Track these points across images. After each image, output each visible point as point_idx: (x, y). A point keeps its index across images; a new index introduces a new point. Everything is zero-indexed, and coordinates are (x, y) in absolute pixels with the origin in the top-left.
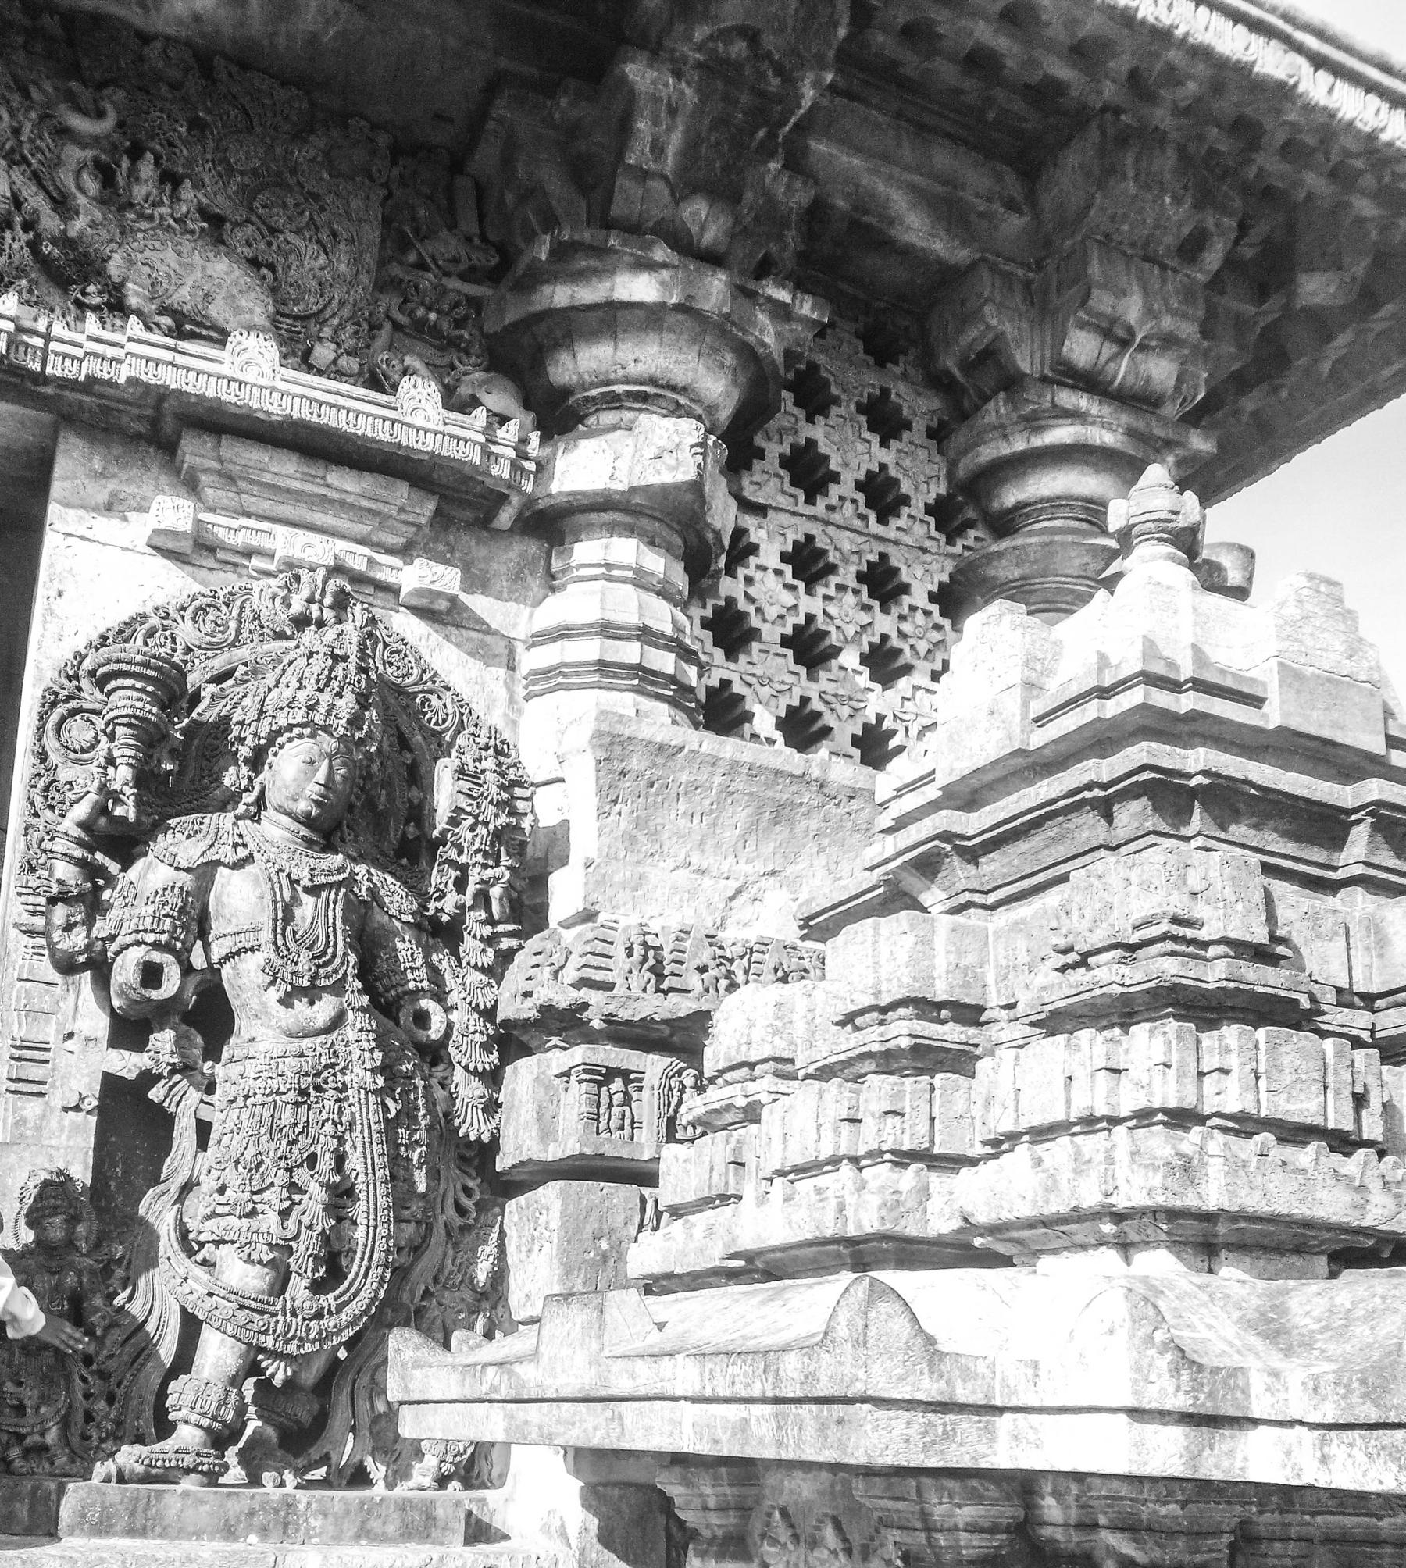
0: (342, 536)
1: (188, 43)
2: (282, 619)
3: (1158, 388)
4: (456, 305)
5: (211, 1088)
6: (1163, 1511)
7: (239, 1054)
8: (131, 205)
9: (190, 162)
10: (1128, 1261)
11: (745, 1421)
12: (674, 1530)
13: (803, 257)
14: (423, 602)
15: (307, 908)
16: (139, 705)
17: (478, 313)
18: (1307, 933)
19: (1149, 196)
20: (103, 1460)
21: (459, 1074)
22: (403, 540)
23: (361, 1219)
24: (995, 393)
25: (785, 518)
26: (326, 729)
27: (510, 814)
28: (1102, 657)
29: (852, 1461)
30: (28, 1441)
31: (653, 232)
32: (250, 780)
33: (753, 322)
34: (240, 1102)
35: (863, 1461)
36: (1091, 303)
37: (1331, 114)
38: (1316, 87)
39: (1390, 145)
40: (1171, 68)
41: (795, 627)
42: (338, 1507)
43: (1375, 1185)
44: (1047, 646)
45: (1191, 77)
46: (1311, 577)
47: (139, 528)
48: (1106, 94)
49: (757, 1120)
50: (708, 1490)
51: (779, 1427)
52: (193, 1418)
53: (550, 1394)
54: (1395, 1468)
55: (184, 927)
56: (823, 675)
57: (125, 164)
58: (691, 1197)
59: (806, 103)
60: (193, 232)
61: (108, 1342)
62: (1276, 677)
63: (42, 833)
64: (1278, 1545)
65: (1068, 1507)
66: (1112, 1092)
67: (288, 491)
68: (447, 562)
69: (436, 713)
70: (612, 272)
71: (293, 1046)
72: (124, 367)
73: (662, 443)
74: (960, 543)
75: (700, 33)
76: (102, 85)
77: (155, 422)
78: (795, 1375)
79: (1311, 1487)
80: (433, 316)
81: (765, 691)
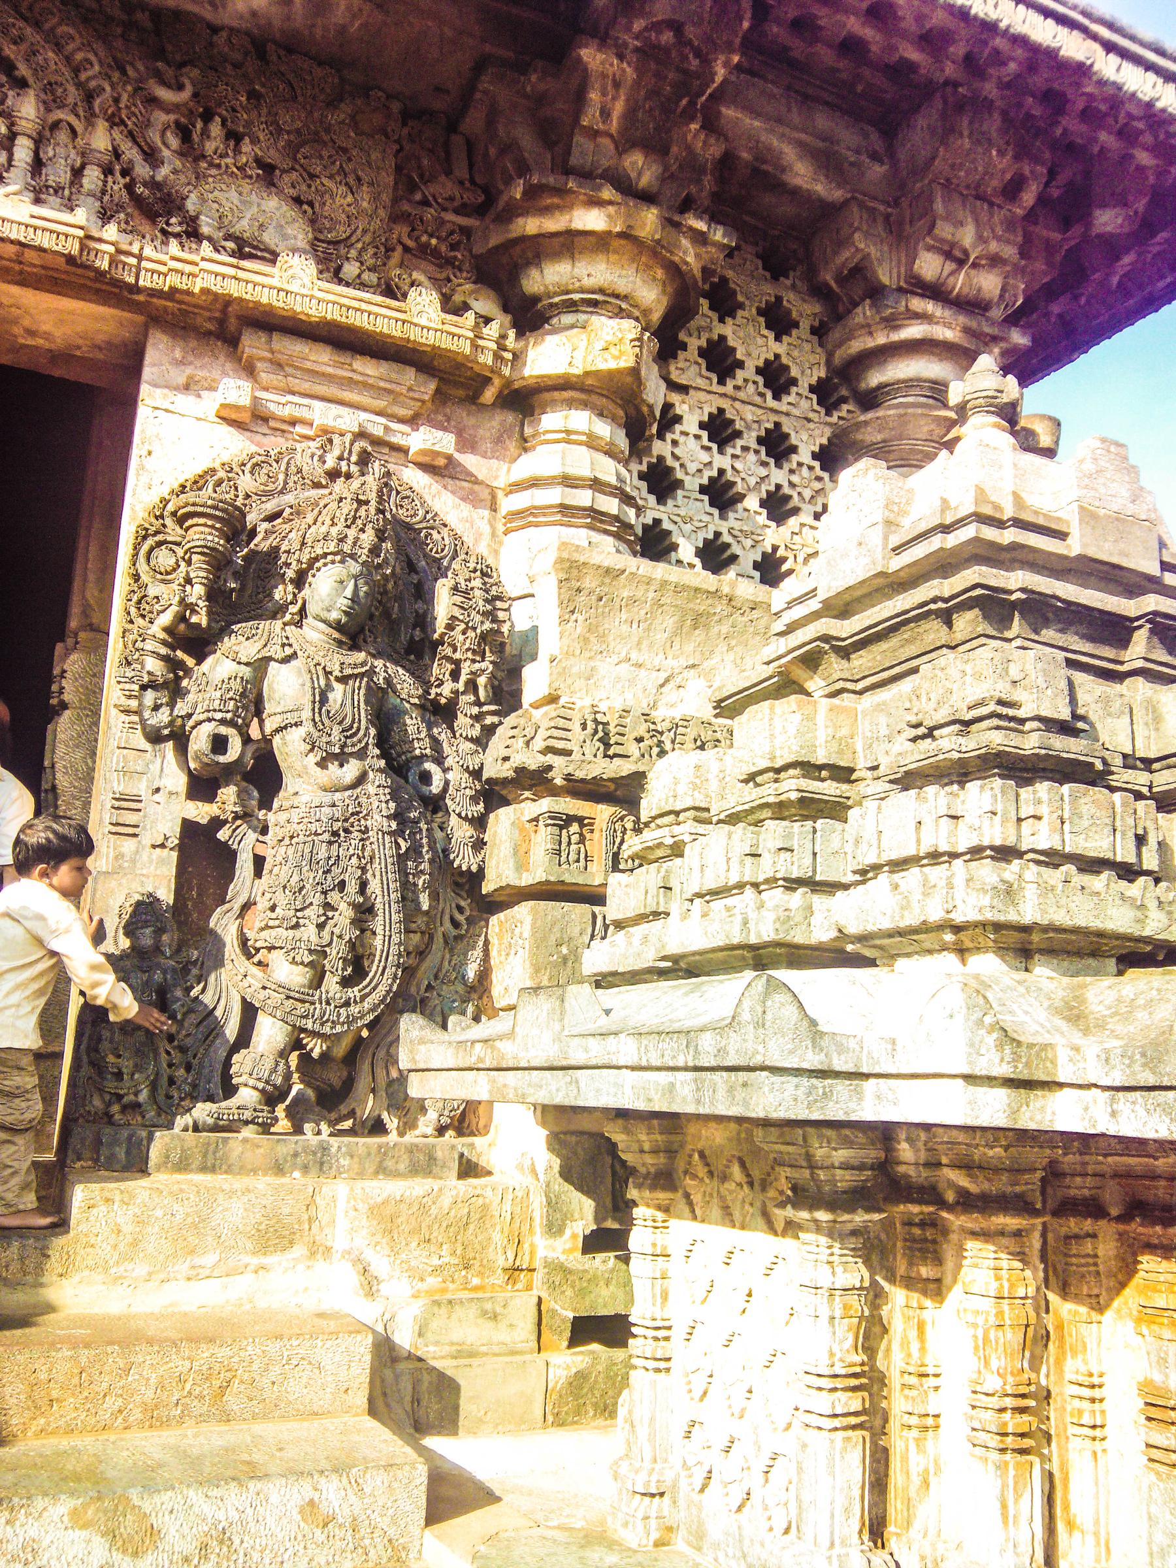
0: (365, 410)
1: (248, 33)
2: (319, 473)
3: (987, 296)
4: (452, 233)
5: (264, 831)
6: (991, 1153)
7: (286, 804)
8: (204, 157)
9: (248, 124)
10: (964, 962)
11: (672, 1085)
12: (618, 1167)
13: (716, 196)
14: (426, 459)
15: (338, 693)
16: (210, 538)
17: (468, 239)
18: (1101, 712)
19: (980, 150)
20: (182, 1114)
21: (454, 820)
22: (411, 412)
23: (379, 930)
24: (863, 300)
25: (702, 396)
26: (353, 556)
27: (493, 621)
28: (944, 501)
29: (753, 1115)
30: (125, 1100)
31: (602, 177)
32: (295, 595)
33: (679, 247)
34: (287, 841)
35: (762, 1115)
36: (936, 231)
37: (1118, 87)
38: (1108, 67)
39: (1163, 110)
40: (996, 52)
41: (710, 478)
42: (361, 1150)
43: (1152, 904)
44: (902, 493)
45: (1012, 59)
46: (1103, 440)
47: (210, 403)
48: (947, 71)
49: (682, 856)
50: (643, 1137)
51: (698, 1089)
52: (251, 1082)
53: (524, 1064)
54: (1168, 1121)
55: (245, 707)
56: (731, 515)
57: (199, 125)
58: (630, 914)
59: (719, 79)
60: (250, 177)
61: (186, 1024)
62: (1077, 517)
63: (135, 636)
64: (1078, 1179)
65: (918, 1150)
66: (952, 833)
67: (323, 374)
68: (445, 429)
69: (435, 543)
70: (571, 207)
71: (327, 798)
72: (198, 280)
73: (610, 338)
74: (836, 414)
75: (638, 25)
76: (183, 65)
77: (222, 322)
78: (710, 1049)
79: (1103, 1135)
80: (434, 241)
81: (688, 528)
